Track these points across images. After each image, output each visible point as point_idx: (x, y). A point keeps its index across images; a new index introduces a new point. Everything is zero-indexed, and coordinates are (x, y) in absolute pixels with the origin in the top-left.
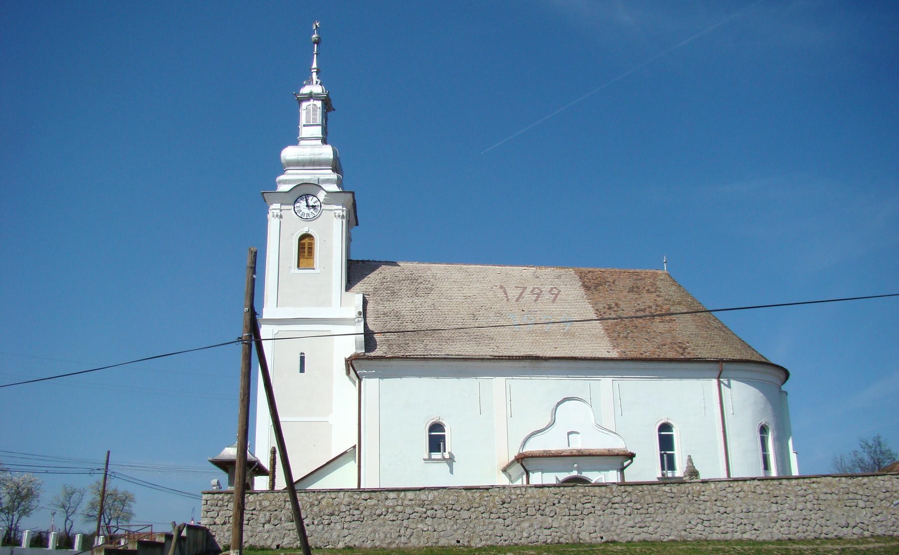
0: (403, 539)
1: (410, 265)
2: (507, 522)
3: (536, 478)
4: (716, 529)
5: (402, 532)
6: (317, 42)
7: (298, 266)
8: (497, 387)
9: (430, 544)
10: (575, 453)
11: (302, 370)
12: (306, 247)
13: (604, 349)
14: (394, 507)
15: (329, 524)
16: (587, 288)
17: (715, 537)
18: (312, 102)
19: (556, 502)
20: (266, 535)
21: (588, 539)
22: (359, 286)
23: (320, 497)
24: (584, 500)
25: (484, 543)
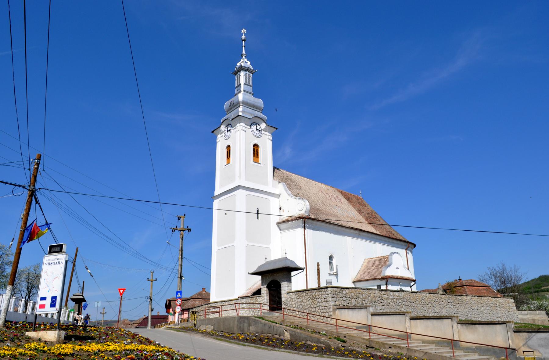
1: (284, 172)
6: (244, 40)
11: (258, 218)
18: (247, 72)
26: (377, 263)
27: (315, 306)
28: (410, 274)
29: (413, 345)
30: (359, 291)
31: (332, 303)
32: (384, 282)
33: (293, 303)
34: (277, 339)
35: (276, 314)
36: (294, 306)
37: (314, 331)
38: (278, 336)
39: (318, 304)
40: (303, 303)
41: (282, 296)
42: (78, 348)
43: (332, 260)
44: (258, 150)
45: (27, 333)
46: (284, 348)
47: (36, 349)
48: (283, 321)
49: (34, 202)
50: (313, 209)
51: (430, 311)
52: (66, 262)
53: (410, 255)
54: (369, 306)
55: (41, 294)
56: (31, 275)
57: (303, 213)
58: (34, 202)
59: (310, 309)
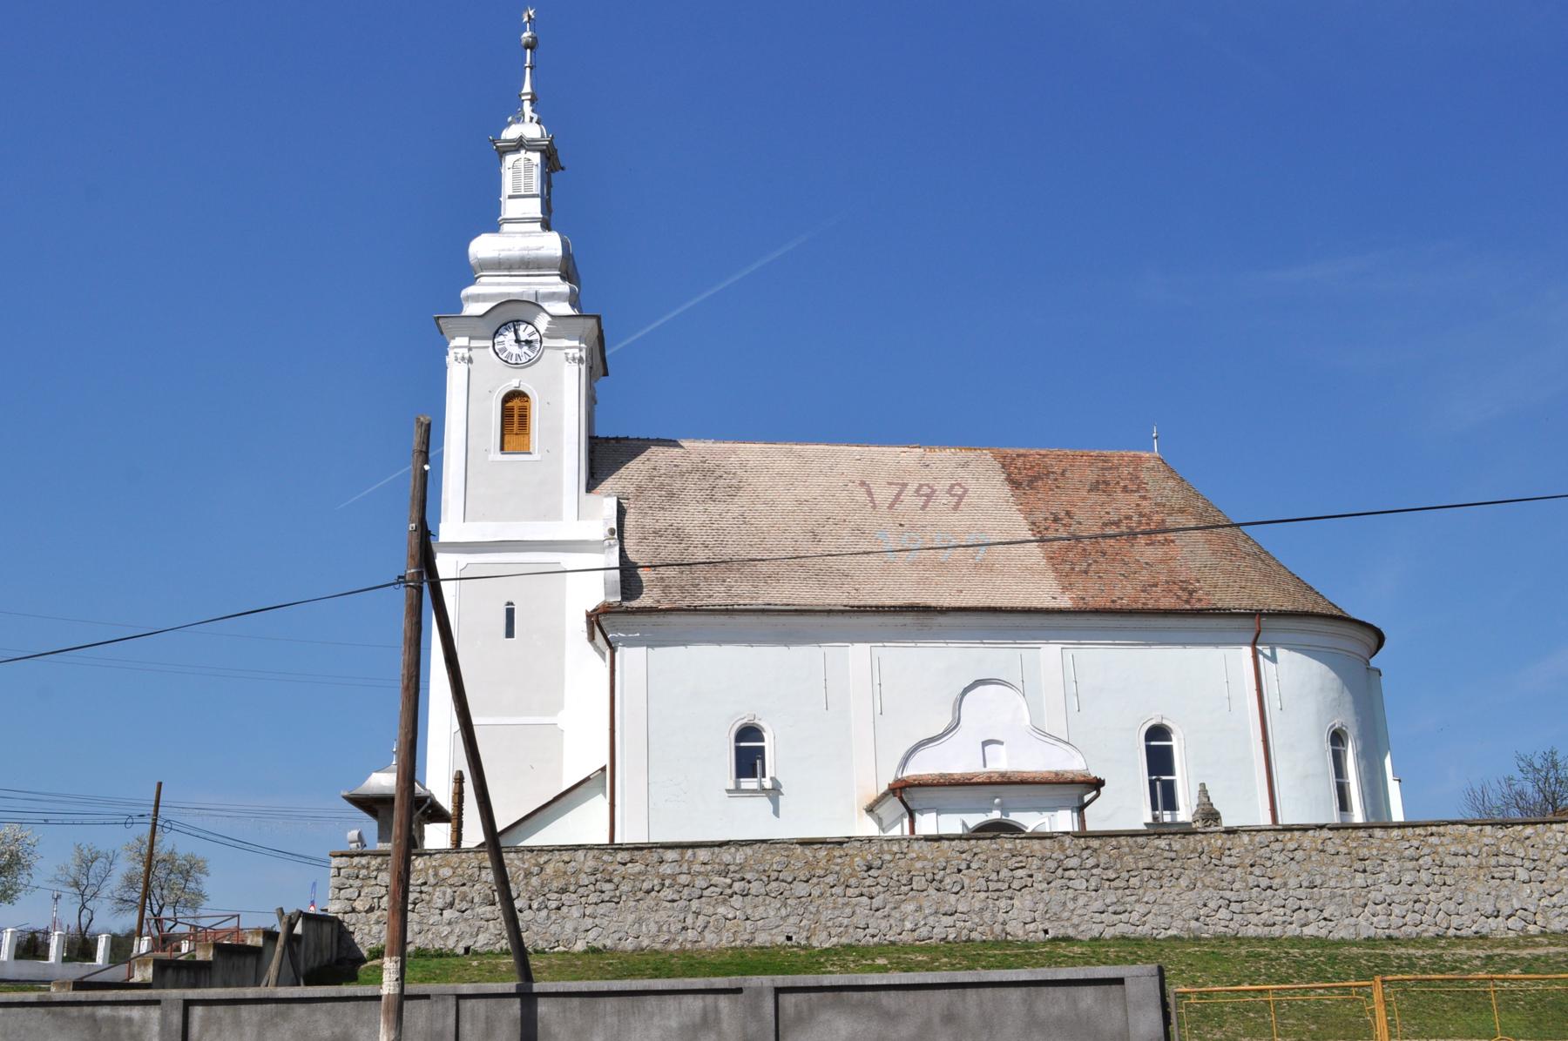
0: (691, 934)
2: (877, 902)
3: (928, 824)
4: (1254, 919)
5: (689, 921)
6: (531, 46)
7: (502, 449)
8: (855, 660)
9: (738, 943)
10: (995, 778)
11: (510, 633)
12: (514, 414)
13: (1045, 592)
14: (674, 876)
15: (558, 908)
16: (1015, 484)
17: (1251, 931)
19: (963, 866)
20: (446, 930)
21: (1021, 933)
22: (609, 484)
23: (542, 860)
24: (1012, 863)
25: (835, 940)
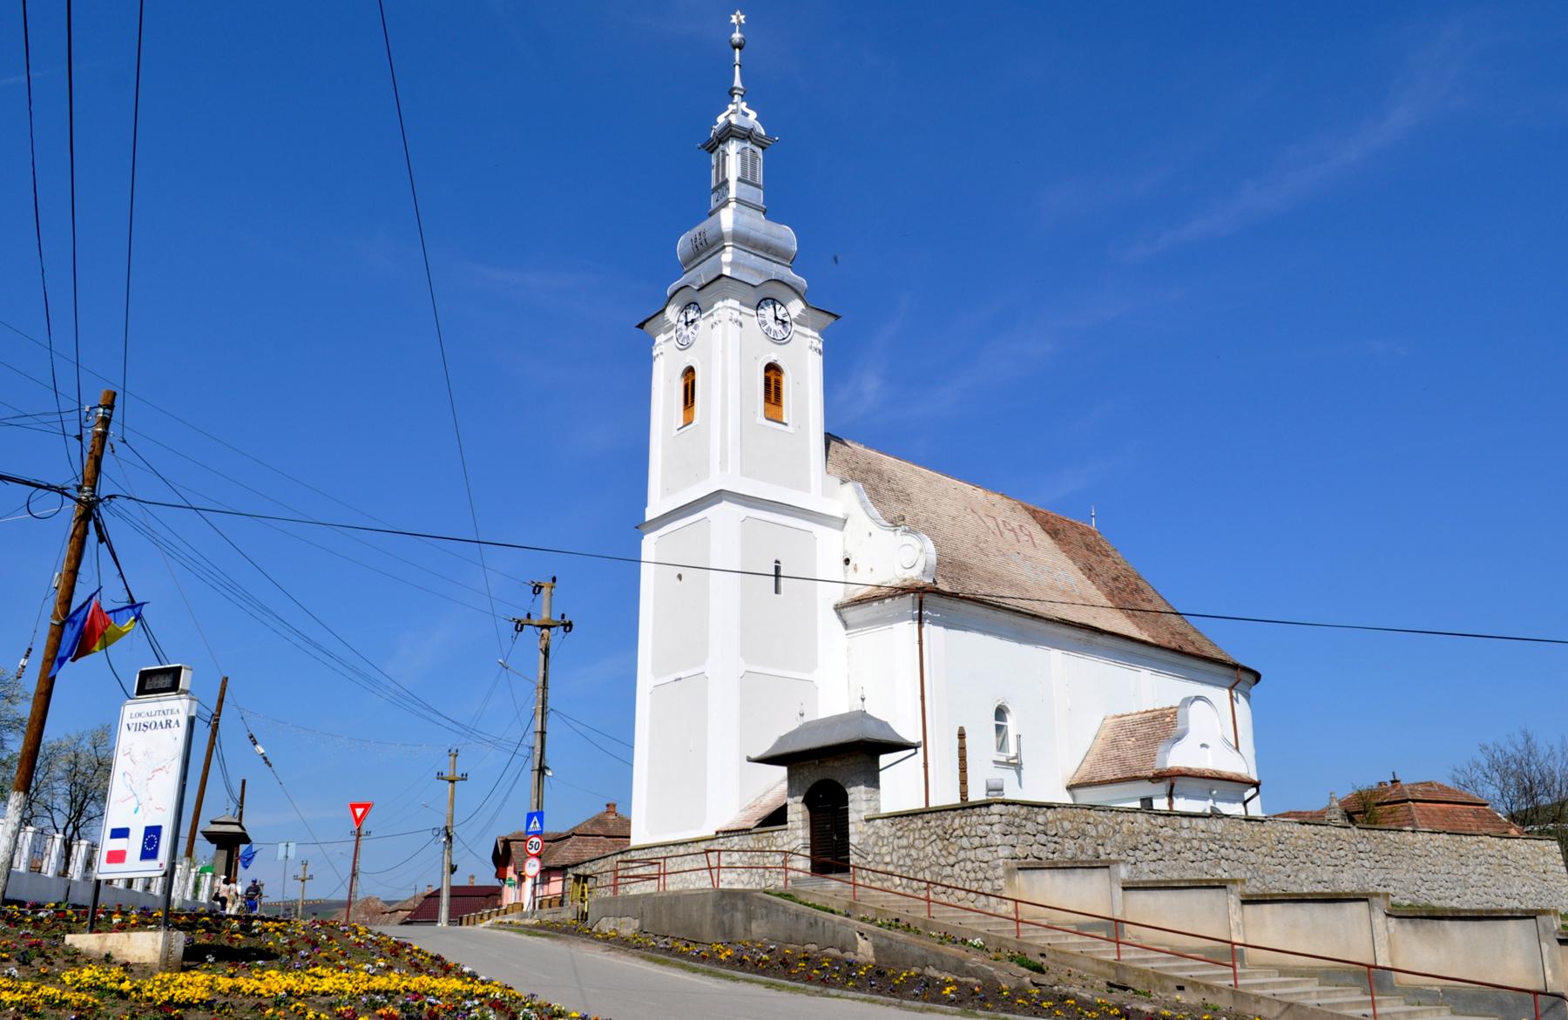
1: (860, 448)
6: (740, 47)
11: (777, 592)
18: (748, 145)
26: (1143, 730)
27: (952, 860)
28: (1242, 765)
29: (1251, 981)
30: (1087, 816)
31: (1004, 852)
32: (1162, 787)
33: (884, 850)
34: (836, 960)
35: (833, 885)
36: (887, 859)
37: (946, 938)
38: (835, 952)
39: (962, 855)
40: (913, 852)
41: (852, 828)
42: (224, 983)
43: (1004, 720)
44: (778, 382)
45: (69, 938)
46: (857, 988)
47: (97, 988)
48: (852, 905)
49: (92, 536)
50: (945, 563)
51: (1303, 876)
52: (191, 721)
53: (1243, 707)
54: (1116, 862)
55: (113, 820)
56: (83, 759)
57: (915, 575)
58: (92, 536)
59: (936, 869)
